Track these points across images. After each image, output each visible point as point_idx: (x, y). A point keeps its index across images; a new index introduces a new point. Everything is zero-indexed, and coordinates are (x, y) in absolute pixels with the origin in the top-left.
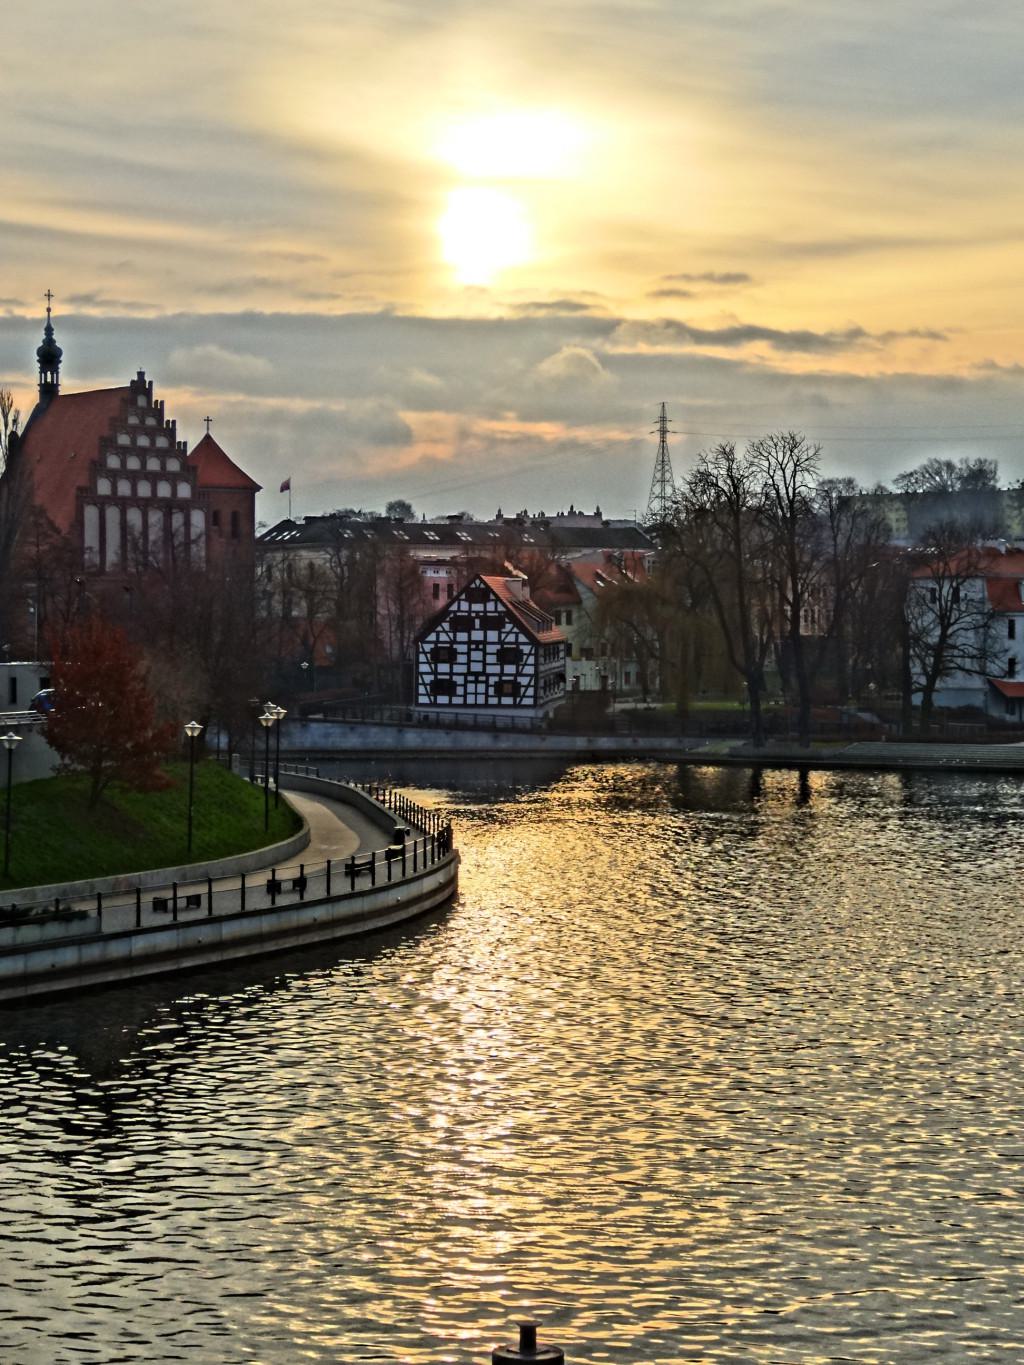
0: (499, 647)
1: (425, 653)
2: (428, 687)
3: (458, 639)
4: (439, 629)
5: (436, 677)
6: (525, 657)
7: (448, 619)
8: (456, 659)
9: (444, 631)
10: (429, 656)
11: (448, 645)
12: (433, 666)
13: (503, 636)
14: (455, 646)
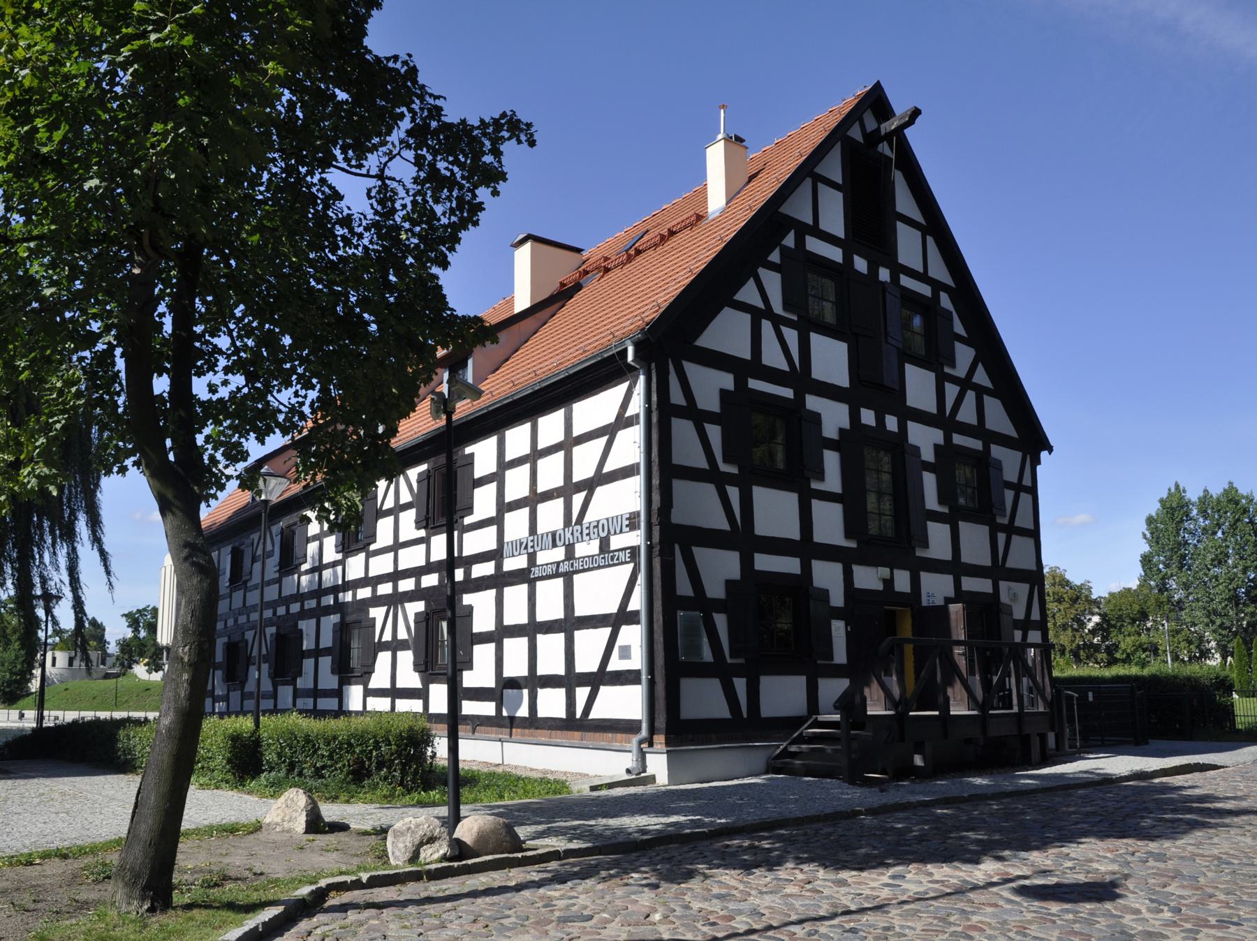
0: (937, 436)
1: (699, 418)
2: (721, 620)
3: (818, 373)
4: (748, 294)
5: (747, 563)
6: (1009, 495)
7: (775, 257)
8: (821, 476)
9: (768, 313)
10: (714, 433)
11: (788, 393)
12: (734, 493)
13: (951, 391)
14: (813, 403)
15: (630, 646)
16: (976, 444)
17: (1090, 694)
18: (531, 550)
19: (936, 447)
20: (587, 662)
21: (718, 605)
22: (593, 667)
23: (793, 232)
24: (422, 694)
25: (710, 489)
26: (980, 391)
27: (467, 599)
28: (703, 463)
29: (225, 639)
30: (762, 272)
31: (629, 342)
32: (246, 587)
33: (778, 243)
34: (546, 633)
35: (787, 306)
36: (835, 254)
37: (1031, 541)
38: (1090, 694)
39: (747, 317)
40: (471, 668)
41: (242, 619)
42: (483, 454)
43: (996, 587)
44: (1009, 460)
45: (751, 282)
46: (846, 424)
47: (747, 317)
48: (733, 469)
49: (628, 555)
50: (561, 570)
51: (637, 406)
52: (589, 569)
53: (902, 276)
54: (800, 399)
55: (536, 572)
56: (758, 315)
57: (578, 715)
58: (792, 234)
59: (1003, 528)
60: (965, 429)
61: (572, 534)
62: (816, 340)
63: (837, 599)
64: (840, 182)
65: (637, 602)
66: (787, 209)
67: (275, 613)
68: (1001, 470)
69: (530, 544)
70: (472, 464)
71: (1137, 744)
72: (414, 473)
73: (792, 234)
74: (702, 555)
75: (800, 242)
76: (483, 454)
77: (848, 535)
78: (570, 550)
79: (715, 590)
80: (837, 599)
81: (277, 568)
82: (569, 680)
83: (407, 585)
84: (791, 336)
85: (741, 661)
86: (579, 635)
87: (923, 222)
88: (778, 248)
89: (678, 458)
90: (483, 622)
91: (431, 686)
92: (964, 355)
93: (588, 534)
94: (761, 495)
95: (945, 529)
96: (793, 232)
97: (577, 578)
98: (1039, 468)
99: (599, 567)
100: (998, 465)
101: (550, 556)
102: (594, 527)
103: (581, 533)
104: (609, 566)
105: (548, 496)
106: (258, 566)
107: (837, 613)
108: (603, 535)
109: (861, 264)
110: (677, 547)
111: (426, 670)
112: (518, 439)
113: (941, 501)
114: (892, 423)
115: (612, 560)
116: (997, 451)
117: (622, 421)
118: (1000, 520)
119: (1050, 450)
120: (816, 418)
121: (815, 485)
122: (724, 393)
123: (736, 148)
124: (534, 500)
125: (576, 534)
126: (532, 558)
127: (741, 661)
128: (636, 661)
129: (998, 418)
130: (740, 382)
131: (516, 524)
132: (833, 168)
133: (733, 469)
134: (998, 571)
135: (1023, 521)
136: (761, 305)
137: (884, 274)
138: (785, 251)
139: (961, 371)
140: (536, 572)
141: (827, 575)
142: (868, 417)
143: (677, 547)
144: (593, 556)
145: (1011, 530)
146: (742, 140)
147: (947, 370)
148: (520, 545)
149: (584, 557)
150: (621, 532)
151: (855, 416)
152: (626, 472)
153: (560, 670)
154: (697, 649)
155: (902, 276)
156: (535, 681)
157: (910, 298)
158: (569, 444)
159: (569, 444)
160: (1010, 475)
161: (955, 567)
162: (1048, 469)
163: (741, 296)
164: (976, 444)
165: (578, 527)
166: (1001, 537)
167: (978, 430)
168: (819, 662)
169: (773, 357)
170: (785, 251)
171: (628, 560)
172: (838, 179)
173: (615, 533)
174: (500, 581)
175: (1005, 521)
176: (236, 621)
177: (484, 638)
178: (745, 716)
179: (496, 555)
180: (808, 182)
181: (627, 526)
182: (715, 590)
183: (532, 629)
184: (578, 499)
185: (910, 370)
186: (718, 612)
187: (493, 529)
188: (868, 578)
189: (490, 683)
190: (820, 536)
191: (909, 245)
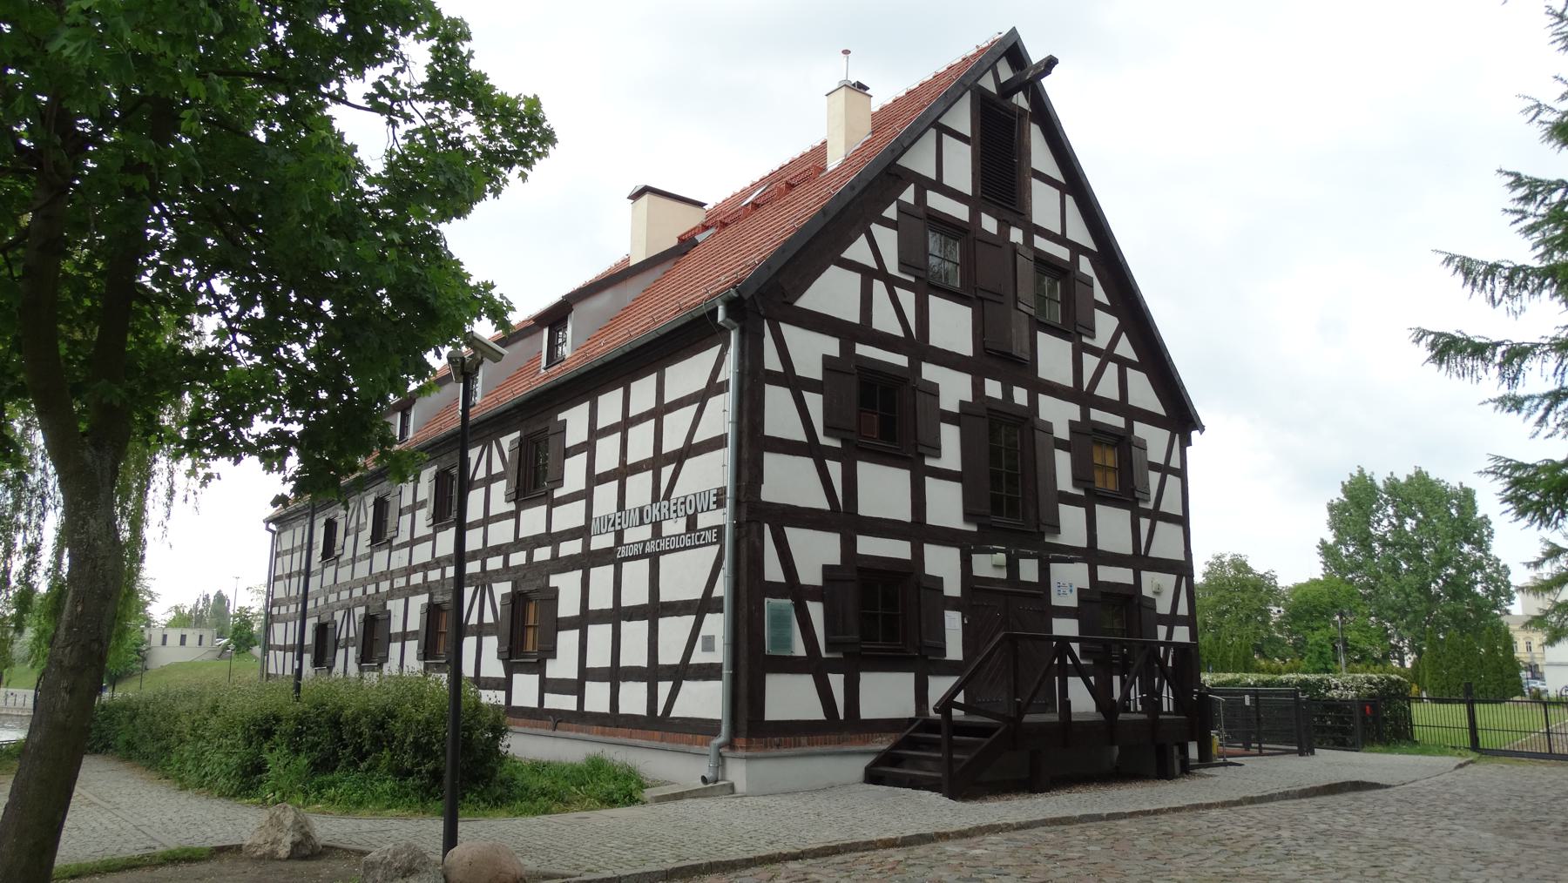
0: (1073, 411)
1: (797, 385)
2: (816, 610)
3: (937, 339)
4: (859, 251)
5: (848, 546)
6: (1154, 478)
7: (891, 212)
8: (936, 451)
9: (881, 273)
10: (814, 402)
11: (901, 360)
12: (835, 469)
13: (1090, 363)
14: (930, 372)
15: (714, 636)
16: (1118, 422)
17: (1247, 698)
18: (618, 528)
19: (1071, 422)
20: (670, 655)
21: (814, 593)
22: (676, 660)
23: (913, 185)
24: (506, 685)
25: (807, 464)
26: (1123, 363)
27: (555, 580)
28: (800, 435)
29: (315, 620)
30: (875, 228)
31: (718, 302)
32: (338, 563)
33: (894, 197)
34: (629, 620)
35: (903, 265)
36: (961, 212)
37: (1179, 530)
38: (1247, 698)
39: (858, 276)
40: (554, 657)
41: (333, 598)
42: (575, 422)
43: (1137, 578)
44: (1155, 441)
45: (863, 239)
46: (969, 398)
47: (856, 278)
48: (836, 444)
49: (714, 535)
50: (647, 550)
51: (729, 372)
52: (675, 550)
53: (1036, 237)
54: (915, 369)
55: (623, 552)
56: (868, 275)
57: (659, 714)
58: (911, 188)
59: (1147, 514)
60: (1105, 405)
61: (659, 511)
62: (935, 302)
63: (953, 588)
64: (968, 133)
65: (721, 589)
66: (906, 162)
67: (364, 592)
68: (1145, 449)
69: (618, 521)
70: (564, 431)
71: (1301, 754)
72: (506, 441)
73: (911, 188)
74: (796, 537)
75: (920, 197)
76: (575, 422)
77: (968, 517)
78: (657, 527)
79: (810, 575)
80: (953, 588)
81: (369, 542)
82: (652, 673)
83: (495, 563)
84: (907, 299)
85: (839, 655)
86: (663, 623)
87: (1062, 180)
88: (895, 202)
89: (771, 428)
90: (568, 606)
91: (516, 677)
92: (1106, 325)
93: (675, 511)
94: (865, 470)
95: (1080, 513)
96: (913, 185)
97: (663, 559)
98: (1188, 449)
99: (685, 548)
100: (1143, 446)
101: (638, 534)
102: (682, 503)
103: (669, 509)
104: (696, 547)
105: (638, 468)
106: (351, 539)
107: (954, 604)
108: (690, 512)
109: (989, 224)
110: (767, 527)
111: (510, 658)
112: (610, 406)
113: (1077, 481)
114: (1020, 396)
115: (699, 537)
116: (1141, 429)
117: (714, 387)
118: (1142, 505)
119: (1202, 429)
120: (933, 390)
121: (929, 462)
122: (827, 360)
123: (857, 95)
124: (624, 472)
125: (664, 510)
126: (619, 536)
127: (839, 655)
128: (719, 655)
129: (1142, 393)
130: (846, 349)
131: (605, 496)
132: (961, 118)
133: (836, 444)
134: (1140, 560)
135: (1170, 505)
136: (873, 264)
137: (1016, 235)
138: (903, 209)
139: (1101, 341)
140: (623, 552)
141: (942, 563)
142: (993, 389)
143: (767, 527)
144: (679, 535)
145: (1157, 515)
146: (867, 88)
147: (1085, 340)
148: (608, 521)
149: (670, 537)
150: (708, 509)
151: (978, 388)
152: (716, 443)
153: (643, 662)
154: (787, 642)
155: (1036, 237)
156: (616, 674)
157: (1044, 263)
158: (659, 412)
159: (659, 412)
160: (1156, 454)
161: (1092, 555)
162: (1200, 449)
163: (848, 254)
164: (1118, 422)
165: (666, 503)
166: (1145, 523)
167: (1120, 406)
168: (930, 658)
169: (885, 320)
170: (903, 209)
171: (714, 540)
172: (965, 128)
173: (702, 511)
174: (586, 561)
175: (1150, 506)
176: (326, 600)
177: (569, 624)
178: (842, 717)
179: (583, 532)
180: (932, 133)
181: (714, 503)
182: (810, 575)
183: (617, 615)
184: (667, 472)
185: (1043, 338)
186: (813, 600)
187: (582, 504)
188: (987, 565)
189: (573, 674)
190: (933, 518)
191: (1045, 205)
